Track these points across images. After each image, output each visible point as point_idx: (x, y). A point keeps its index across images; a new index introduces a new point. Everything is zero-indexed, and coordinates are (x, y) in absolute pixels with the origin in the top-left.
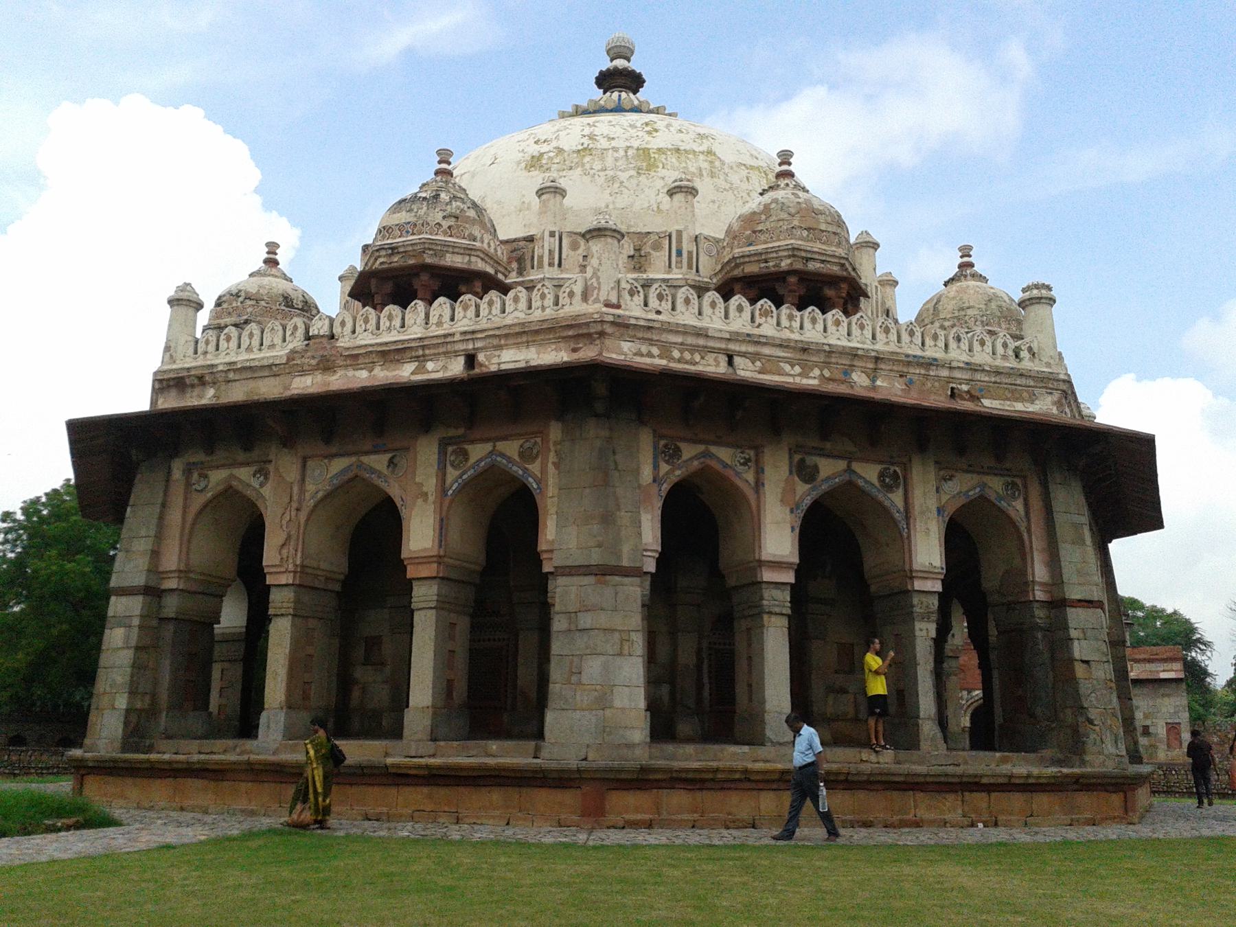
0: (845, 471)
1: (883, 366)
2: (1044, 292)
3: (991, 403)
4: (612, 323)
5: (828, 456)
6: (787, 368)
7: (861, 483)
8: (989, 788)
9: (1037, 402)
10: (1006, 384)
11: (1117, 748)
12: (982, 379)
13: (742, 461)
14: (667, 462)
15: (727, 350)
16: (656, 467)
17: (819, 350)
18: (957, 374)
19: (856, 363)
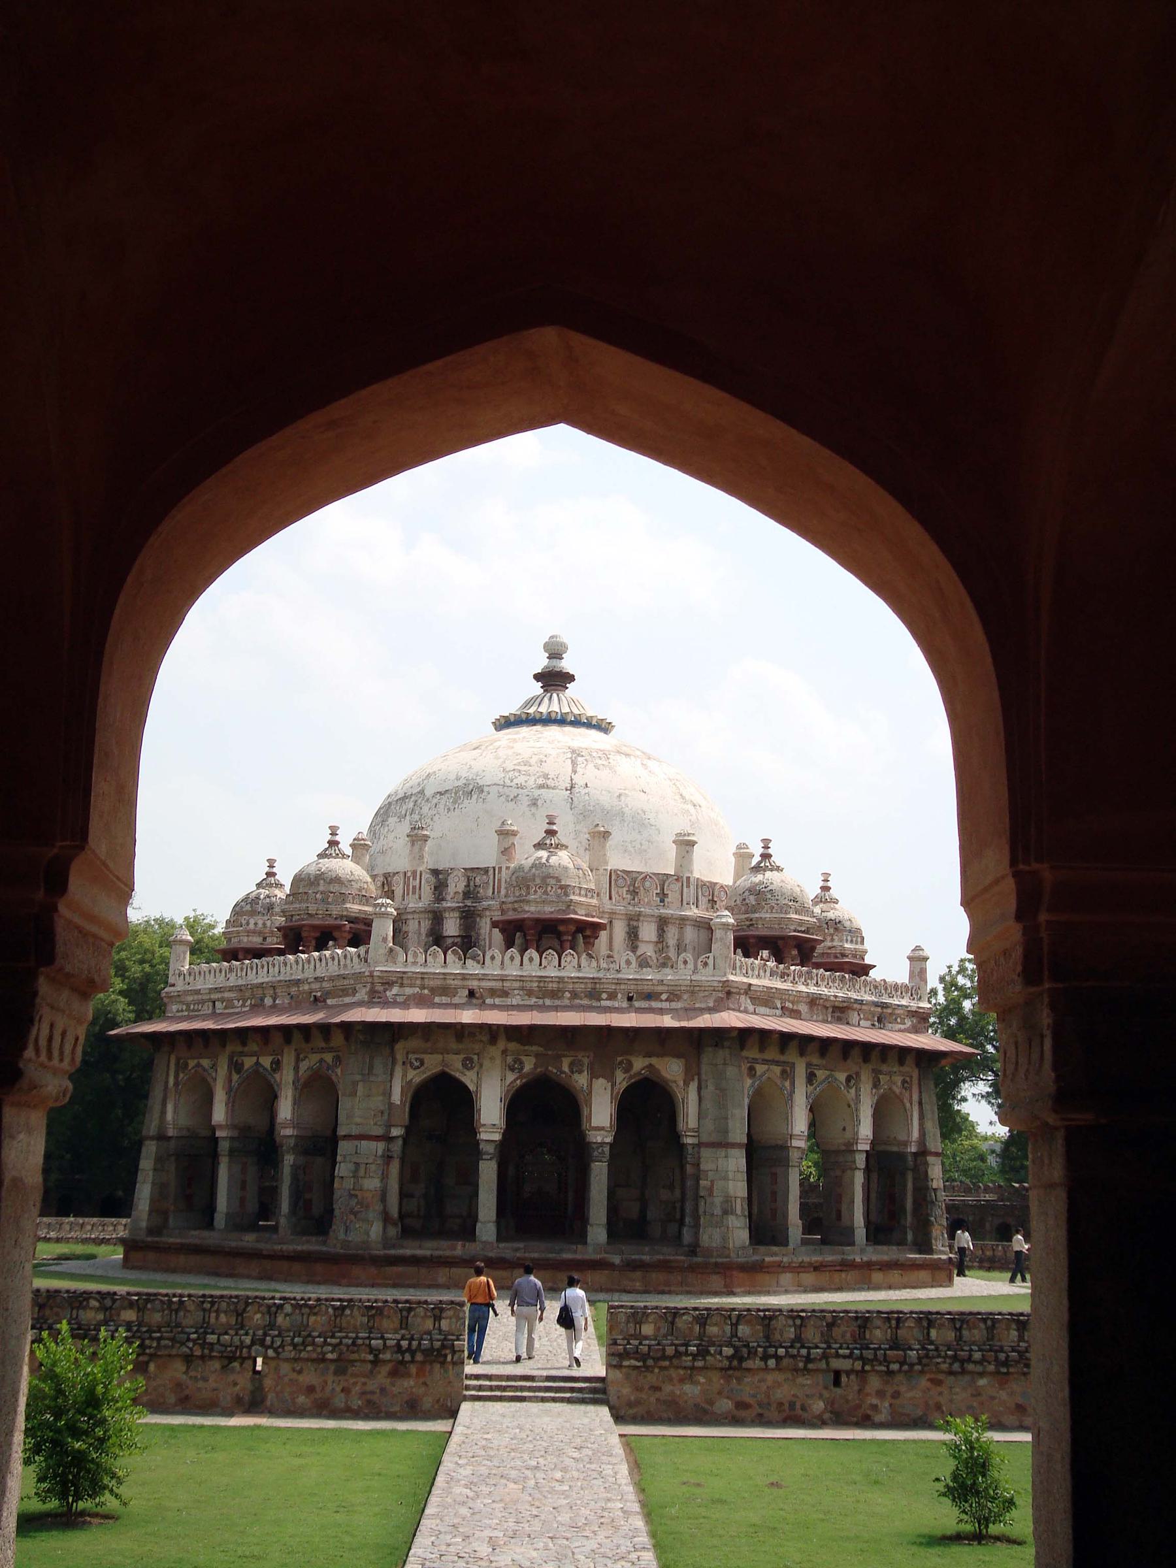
6: (236, 1002)
7: (261, 1070)
9: (357, 995)
11: (346, 1235)
15: (210, 999)
16: (176, 1077)
18: (316, 986)
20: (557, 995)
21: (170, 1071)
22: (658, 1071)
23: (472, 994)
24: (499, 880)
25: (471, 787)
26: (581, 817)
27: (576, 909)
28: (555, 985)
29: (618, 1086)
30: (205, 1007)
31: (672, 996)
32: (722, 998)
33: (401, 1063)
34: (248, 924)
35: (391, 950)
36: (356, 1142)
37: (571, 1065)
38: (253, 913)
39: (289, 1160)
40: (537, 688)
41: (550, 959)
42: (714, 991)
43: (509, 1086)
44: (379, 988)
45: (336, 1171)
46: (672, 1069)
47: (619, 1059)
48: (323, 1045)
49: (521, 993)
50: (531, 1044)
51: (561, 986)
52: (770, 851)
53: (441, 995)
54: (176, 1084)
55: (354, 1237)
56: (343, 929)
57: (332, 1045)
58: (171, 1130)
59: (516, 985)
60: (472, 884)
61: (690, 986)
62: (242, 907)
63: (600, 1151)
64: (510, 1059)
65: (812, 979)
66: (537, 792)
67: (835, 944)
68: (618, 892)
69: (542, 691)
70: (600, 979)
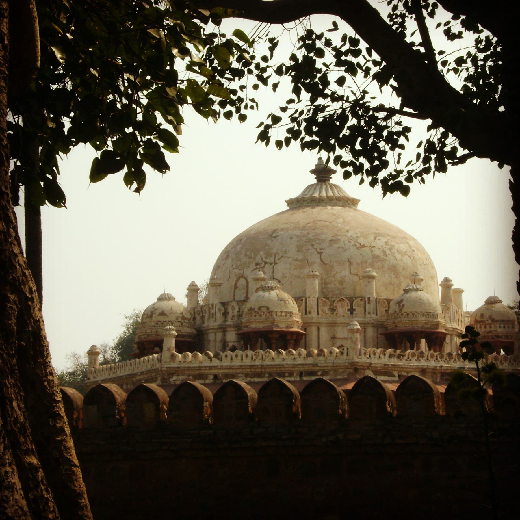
18: (141, 377)
23: (216, 377)
27: (278, 324)
32: (352, 373)
40: (313, 179)
42: (347, 368)
44: (166, 377)
49: (242, 375)
51: (263, 370)
60: (241, 310)
61: (333, 366)
65: (423, 357)
67: (493, 329)
68: (322, 310)
69: (315, 181)
70: (283, 365)
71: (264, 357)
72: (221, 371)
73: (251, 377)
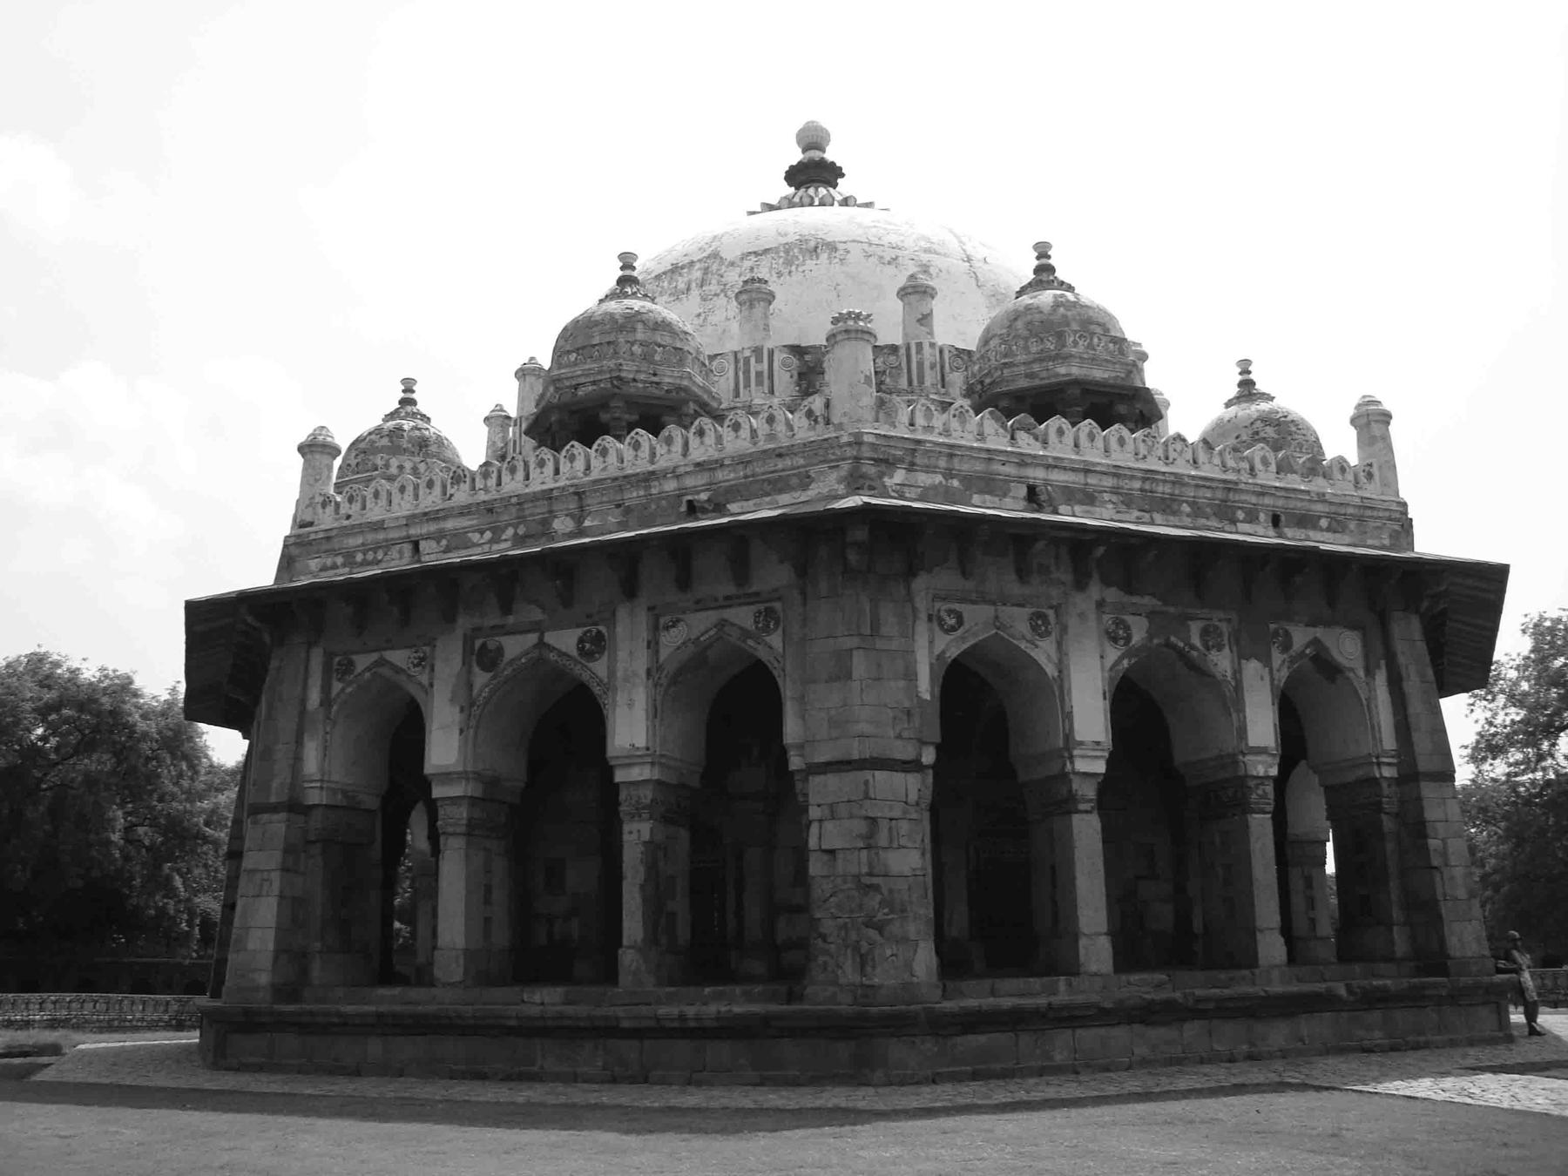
0: (535, 646)
1: (589, 501)
2: (851, 323)
3: (742, 507)
4: (295, 544)
5: (513, 633)
6: (475, 537)
7: (552, 656)
8: (637, 1034)
9: (813, 486)
10: (763, 474)
11: (863, 973)
12: (726, 478)
13: (416, 661)
14: (339, 680)
15: (409, 537)
16: (326, 688)
17: (505, 506)
18: (689, 482)
19: (555, 508)
20: (1169, 506)
21: (310, 681)
22: (1326, 650)
23: (1032, 495)
24: (920, 364)
25: (812, 244)
26: (993, 299)
28: (1168, 489)
29: (1276, 675)
30: (394, 552)
31: (1334, 524)
33: (923, 616)
34: (387, 466)
35: (881, 404)
36: (867, 774)
37: (1205, 633)
38: (395, 450)
39: (636, 834)
41: (1150, 443)
42: (1390, 520)
43: (1111, 669)
44: (870, 469)
45: (813, 843)
46: (1347, 648)
47: (1272, 626)
48: (731, 589)
49: (1114, 498)
50: (1142, 595)
51: (1177, 492)
52: (1252, 376)
53: (981, 492)
54: (326, 702)
55: (883, 977)
56: (685, 409)
57: (754, 589)
58: (317, 791)
59: (1109, 482)
62: (374, 442)
63: (1260, 792)
64: (1107, 619)
66: (925, 257)
70: (1236, 483)
71: (1172, 455)
72: (1058, 477)
73: (1140, 510)
